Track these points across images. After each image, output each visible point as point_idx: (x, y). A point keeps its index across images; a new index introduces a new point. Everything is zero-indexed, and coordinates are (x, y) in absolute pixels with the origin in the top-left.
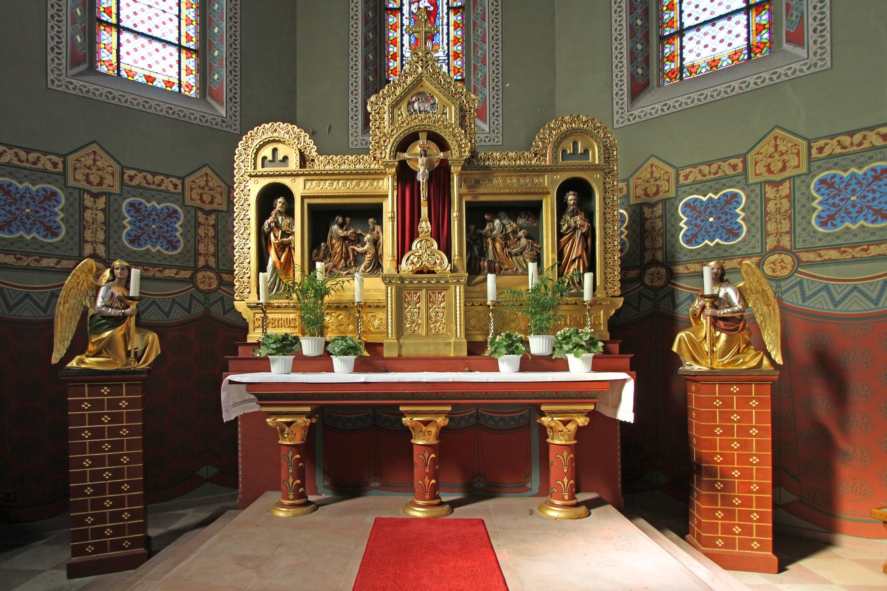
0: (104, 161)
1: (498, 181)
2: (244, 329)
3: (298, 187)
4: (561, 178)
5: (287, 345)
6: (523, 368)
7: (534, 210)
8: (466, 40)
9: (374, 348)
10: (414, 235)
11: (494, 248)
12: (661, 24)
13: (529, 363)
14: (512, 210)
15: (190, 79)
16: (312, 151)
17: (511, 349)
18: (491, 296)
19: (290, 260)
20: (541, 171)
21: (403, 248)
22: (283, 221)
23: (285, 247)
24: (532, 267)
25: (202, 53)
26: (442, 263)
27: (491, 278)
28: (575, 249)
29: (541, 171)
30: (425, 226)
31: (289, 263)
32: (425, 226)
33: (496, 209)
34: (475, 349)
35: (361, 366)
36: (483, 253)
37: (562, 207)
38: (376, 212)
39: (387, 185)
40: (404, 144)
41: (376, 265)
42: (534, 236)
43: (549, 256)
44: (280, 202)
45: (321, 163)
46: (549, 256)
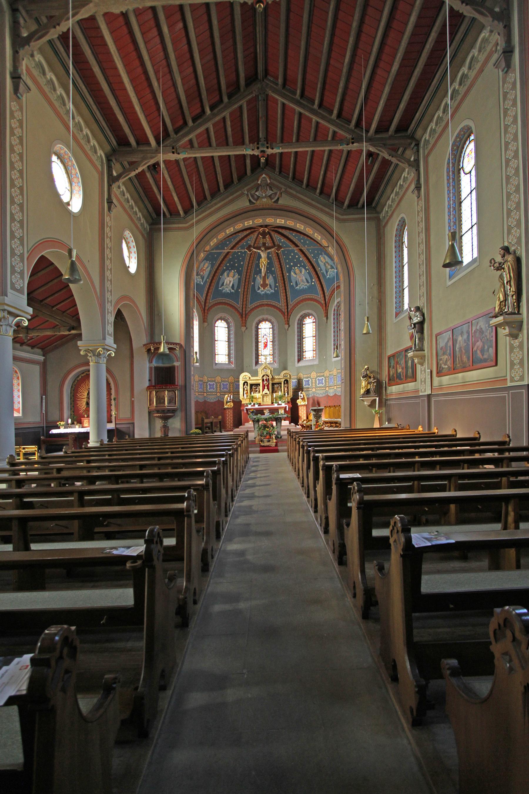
0: (219, 378)
1: (276, 380)
2: (241, 401)
3: (249, 382)
4: (284, 380)
5: (251, 404)
6: (278, 405)
7: (281, 383)
8: (273, 347)
9: (260, 404)
10: (265, 388)
11: (276, 389)
12: (303, 350)
13: (279, 404)
14: (278, 384)
15: (227, 360)
16: (250, 376)
17: (276, 403)
18: (274, 397)
19: (247, 392)
20: (281, 379)
21: (263, 390)
22: (246, 386)
23: (247, 390)
24: (280, 392)
25: (229, 355)
26: (268, 392)
27: (274, 394)
28: (286, 389)
29: (281, 379)
30: (266, 387)
31: (247, 392)
32: (266, 387)
33: (276, 384)
34: (272, 403)
35: (259, 406)
36: (274, 389)
37: (284, 383)
38: (259, 385)
39: (261, 382)
40: (263, 376)
41: (259, 392)
42: (281, 387)
43: (283, 390)
44: (246, 384)
45: (252, 378)
46: (283, 390)
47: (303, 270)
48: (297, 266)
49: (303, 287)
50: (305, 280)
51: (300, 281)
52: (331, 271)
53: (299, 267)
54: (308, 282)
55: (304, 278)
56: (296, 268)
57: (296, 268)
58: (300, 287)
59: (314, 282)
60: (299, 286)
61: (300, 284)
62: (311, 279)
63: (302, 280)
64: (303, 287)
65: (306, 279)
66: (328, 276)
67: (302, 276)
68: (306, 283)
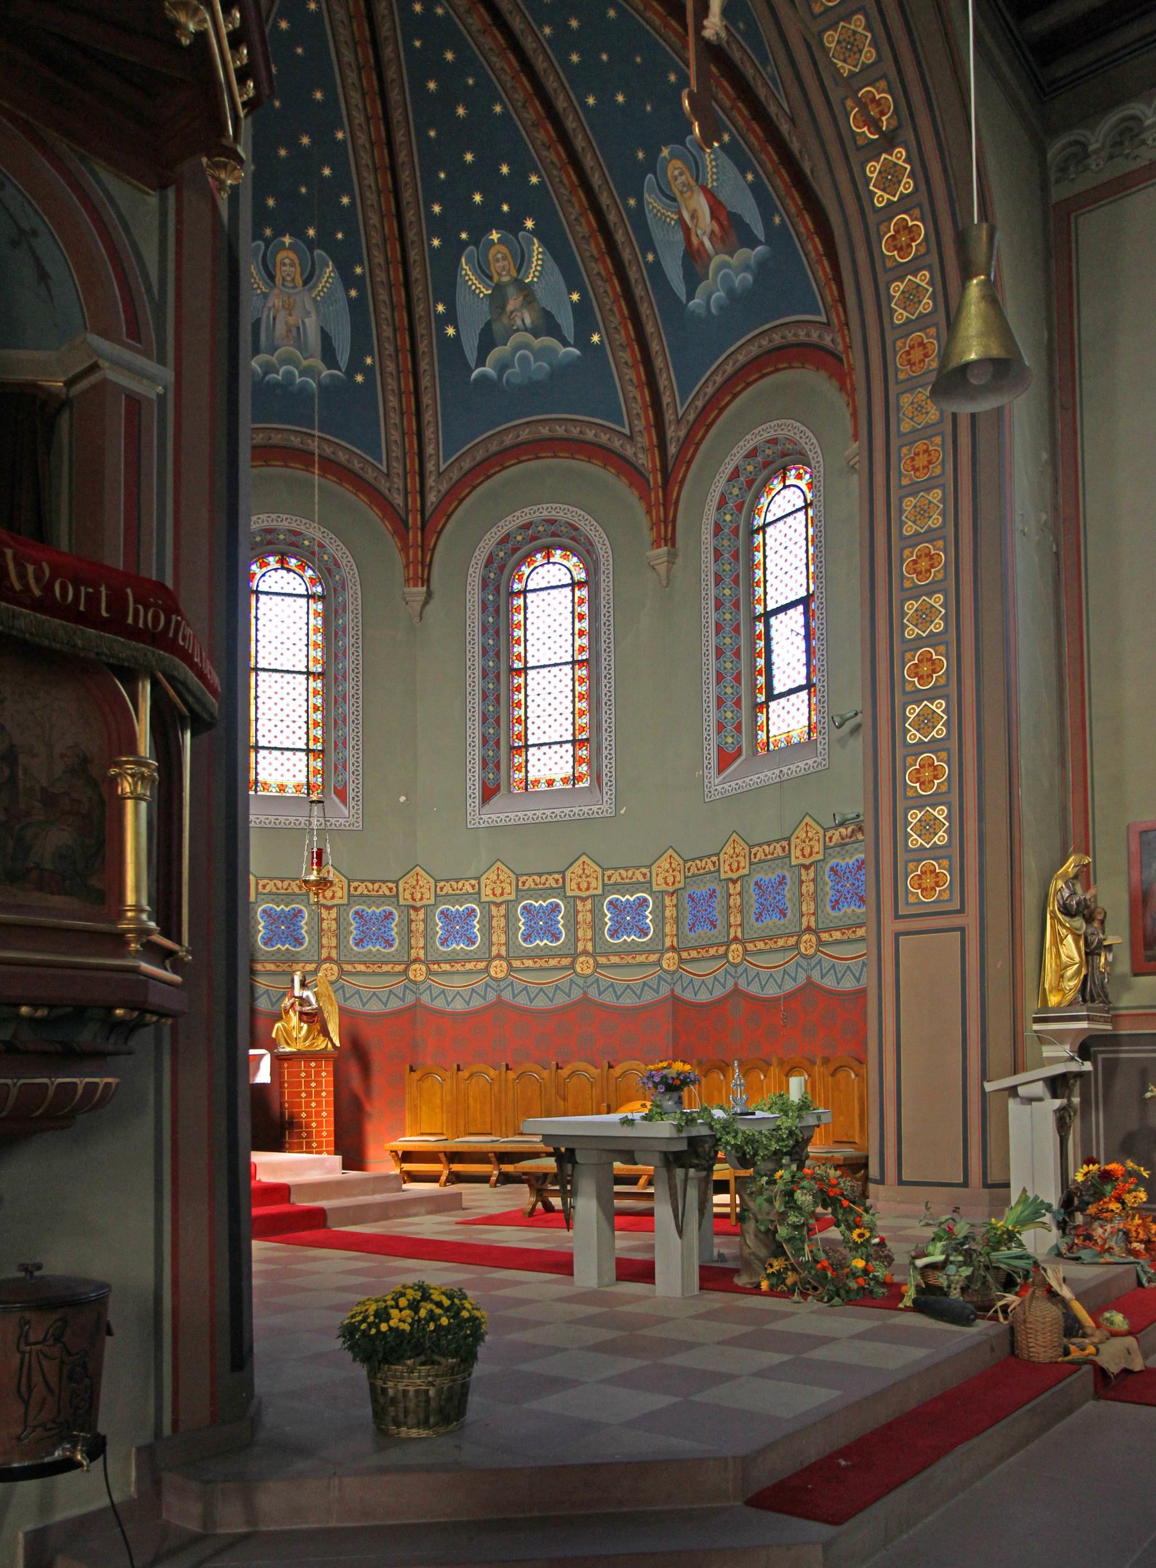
47: (330, 270)
48: (299, 234)
49: (289, 375)
50: (313, 339)
51: (280, 329)
52: (527, 346)
53: (311, 245)
54: (329, 355)
55: (312, 325)
56: (287, 240)
57: (287, 240)
58: (269, 368)
59: (368, 372)
60: (263, 357)
61: (272, 350)
62: (360, 347)
63: (298, 336)
64: (289, 375)
65: (325, 337)
66: (488, 369)
67: (310, 307)
68: (317, 362)
